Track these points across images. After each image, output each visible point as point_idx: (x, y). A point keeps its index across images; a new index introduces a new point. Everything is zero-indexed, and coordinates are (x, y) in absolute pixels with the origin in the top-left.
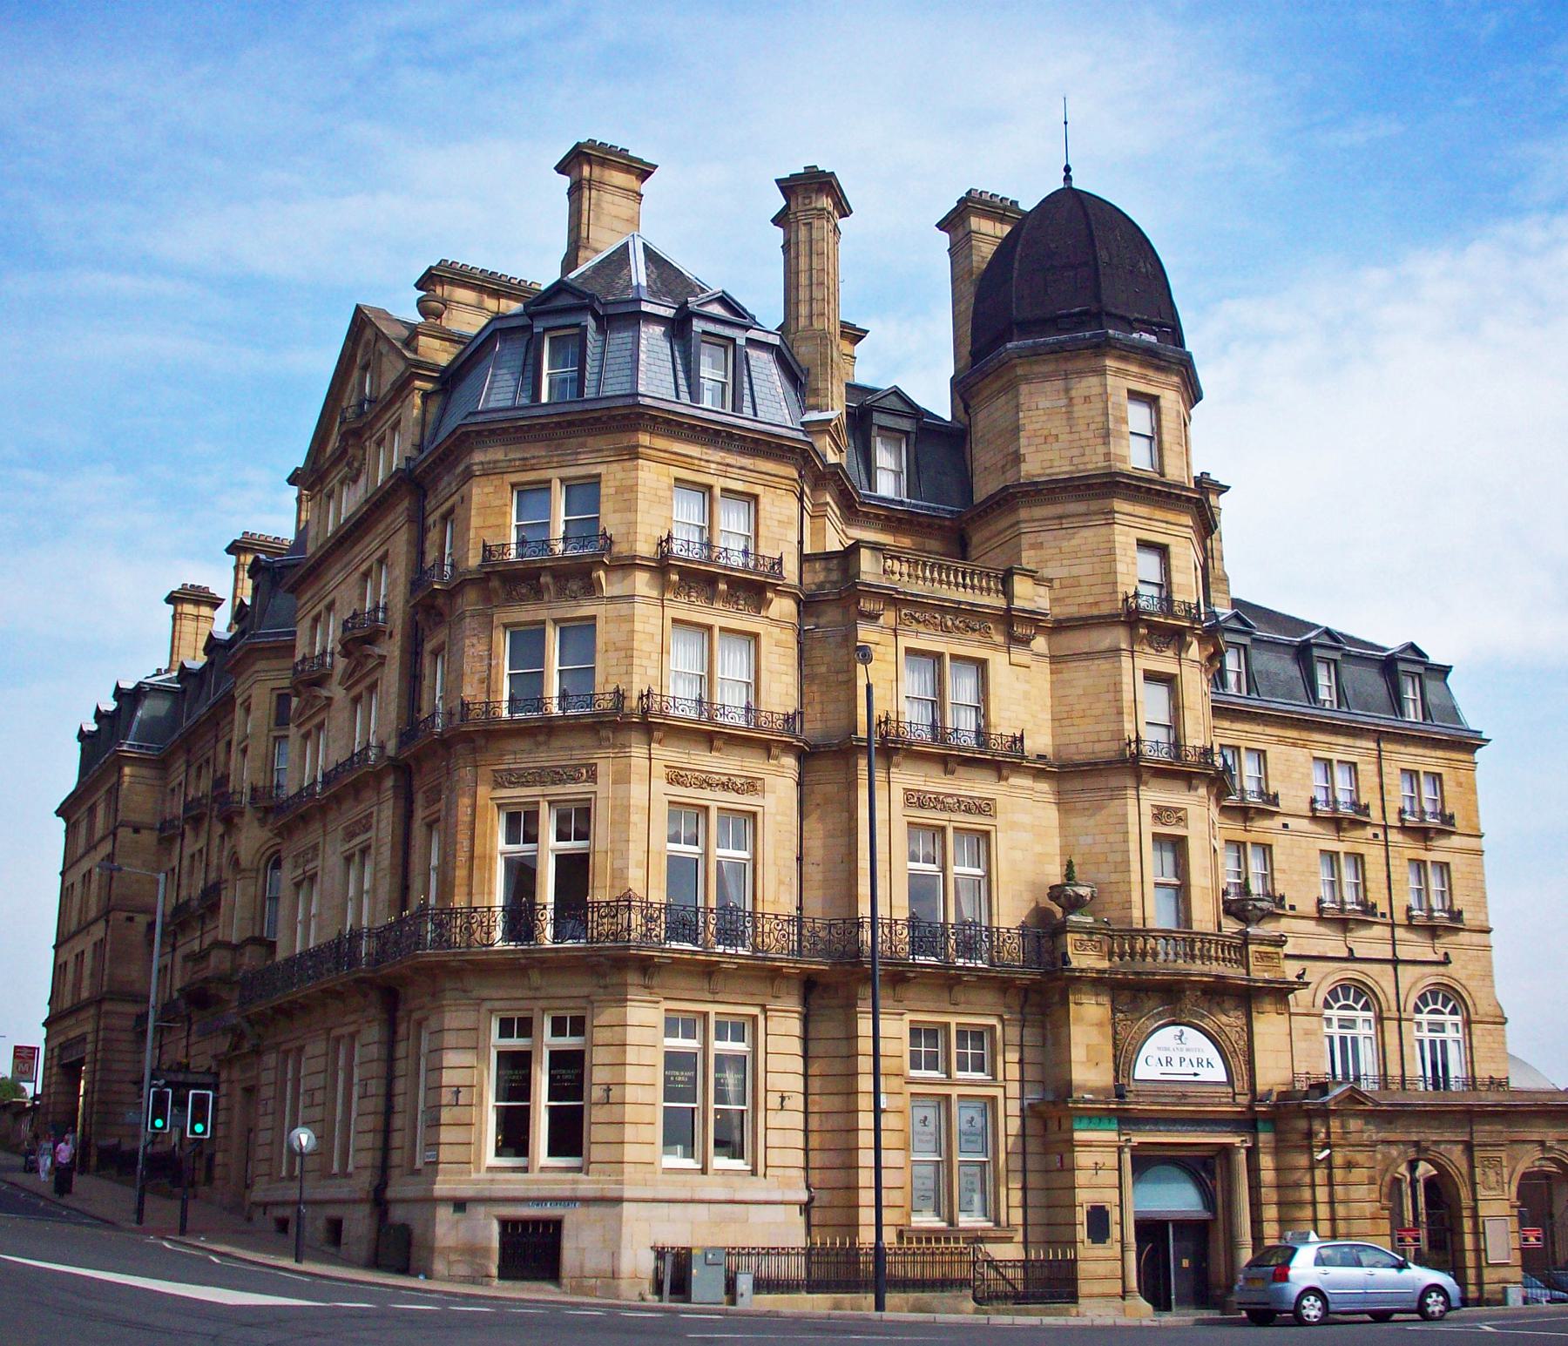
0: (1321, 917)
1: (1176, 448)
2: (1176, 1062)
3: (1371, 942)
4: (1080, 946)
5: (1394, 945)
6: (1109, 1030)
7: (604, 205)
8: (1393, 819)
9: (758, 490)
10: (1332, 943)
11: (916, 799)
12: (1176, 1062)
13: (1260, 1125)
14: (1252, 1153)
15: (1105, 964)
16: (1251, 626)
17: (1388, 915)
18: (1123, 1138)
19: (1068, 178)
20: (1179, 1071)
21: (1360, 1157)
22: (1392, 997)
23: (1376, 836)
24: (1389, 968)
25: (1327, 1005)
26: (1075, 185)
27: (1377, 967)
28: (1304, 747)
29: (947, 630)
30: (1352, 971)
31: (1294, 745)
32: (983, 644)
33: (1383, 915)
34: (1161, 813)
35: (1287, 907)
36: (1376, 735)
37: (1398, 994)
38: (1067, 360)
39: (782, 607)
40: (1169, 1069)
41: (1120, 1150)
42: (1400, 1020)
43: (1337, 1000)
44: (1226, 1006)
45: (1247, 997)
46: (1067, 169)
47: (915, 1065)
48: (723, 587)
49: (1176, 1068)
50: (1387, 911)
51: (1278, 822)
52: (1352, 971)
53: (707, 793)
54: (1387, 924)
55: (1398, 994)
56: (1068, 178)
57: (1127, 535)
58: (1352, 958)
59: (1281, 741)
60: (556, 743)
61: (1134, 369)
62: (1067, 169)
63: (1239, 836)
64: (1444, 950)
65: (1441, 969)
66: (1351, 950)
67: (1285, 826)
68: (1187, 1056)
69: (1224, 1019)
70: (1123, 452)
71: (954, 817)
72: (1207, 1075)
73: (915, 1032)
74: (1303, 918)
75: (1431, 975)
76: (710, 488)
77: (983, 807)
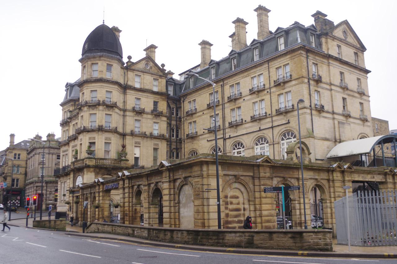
3: (266, 124)
5: (272, 122)
10: (255, 127)
17: (271, 114)
22: (272, 138)
23: (268, 92)
30: (260, 134)
35: (244, 121)
37: (273, 137)
42: (273, 144)
43: (236, 147)
50: (270, 113)
51: (241, 100)
52: (260, 134)
55: (273, 137)
58: (260, 130)
65: (287, 125)
67: (244, 100)
75: (283, 128)
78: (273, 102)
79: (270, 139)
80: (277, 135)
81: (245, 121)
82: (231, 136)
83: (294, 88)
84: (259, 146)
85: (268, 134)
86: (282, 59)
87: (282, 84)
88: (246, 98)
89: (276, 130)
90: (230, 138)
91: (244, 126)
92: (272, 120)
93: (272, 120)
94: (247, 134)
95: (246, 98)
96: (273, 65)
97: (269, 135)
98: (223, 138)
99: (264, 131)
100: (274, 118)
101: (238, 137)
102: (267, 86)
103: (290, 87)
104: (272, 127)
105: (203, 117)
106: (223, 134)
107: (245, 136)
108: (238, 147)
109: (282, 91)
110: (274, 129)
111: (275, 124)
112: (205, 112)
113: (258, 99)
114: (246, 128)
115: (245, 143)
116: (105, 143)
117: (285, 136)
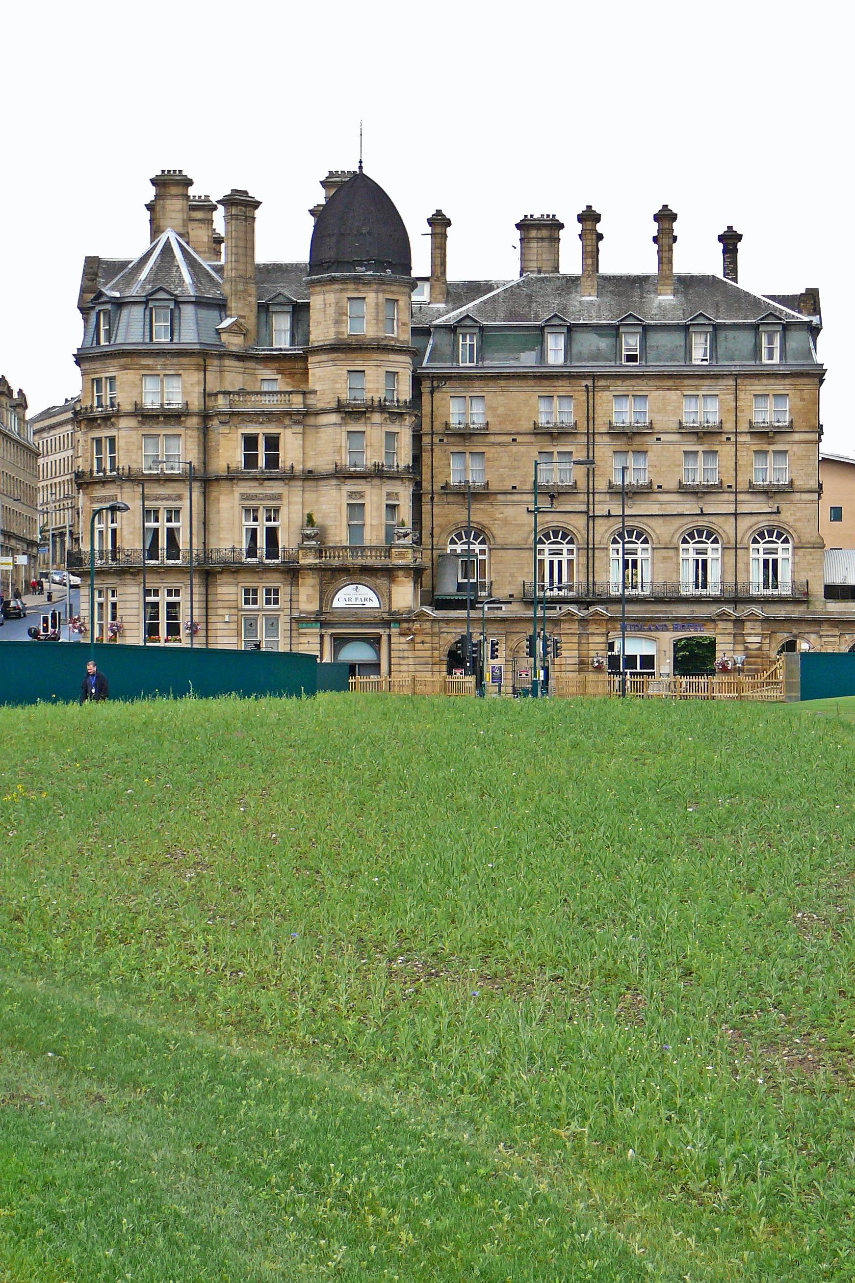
0: (684, 490)
1: (375, 322)
2: (354, 600)
4: (305, 556)
6: (318, 588)
7: (167, 207)
8: (744, 427)
9: (181, 372)
11: (245, 497)
12: (354, 600)
13: (392, 625)
14: (389, 636)
15: (317, 561)
16: (641, 320)
17: (734, 487)
18: (323, 631)
19: (361, 167)
20: (355, 603)
21: (428, 639)
23: (728, 439)
24: (732, 519)
25: (685, 541)
26: (365, 172)
27: (722, 519)
28: (677, 390)
29: (261, 423)
31: (668, 389)
32: (277, 427)
33: (729, 487)
34: (351, 495)
36: (734, 377)
38: (324, 285)
39: (194, 421)
40: (350, 603)
41: (322, 636)
42: (736, 548)
44: (379, 575)
45: (389, 573)
46: (361, 162)
47: (247, 602)
48: (161, 419)
49: (353, 602)
50: (733, 484)
52: (701, 522)
53: (159, 503)
54: (732, 492)
56: (361, 167)
57: (342, 370)
58: (702, 514)
59: (658, 388)
60: (107, 486)
61: (352, 286)
62: (361, 162)
63: (624, 448)
64: (776, 506)
65: (774, 517)
66: (701, 509)
67: (658, 439)
68: (359, 597)
69: (378, 581)
70: (343, 330)
71: (263, 502)
72: (368, 604)
73: (247, 592)
74: (667, 492)
75: (763, 522)
76: (159, 375)
77: (279, 497)
78: (740, 463)
79: (728, 537)
80: (747, 531)
81: (660, 487)
82: (612, 513)
83: (795, 448)
84: (691, 546)
85: (726, 527)
86: (772, 381)
87: (771, 435)
88: (663, 437)
89: (744, 523)
90: (609, 516)
91: (654, 497)
92: (736, 500)
93: (736, 500)
94: (662, 515)
95: (663, 437)
96: (748, 388)
97: (726, 528)
98: (587, 513)
99: (713, 519)
100: (741, 497)
101: (638, 519)
102: (729, 427)
103: (789, 443)
104: (736, 515)
105: (514, 449)
106: (588, 505)
107: (660, 521)
108: (627, 539)
109: (766, 446)
110: (739, 519)
111: (743, 509)
112: (519, 439)
113: (700, 448)
114: (661, 503)
115: (656, 534)
116: (387, 505)
117: (762, 536)
